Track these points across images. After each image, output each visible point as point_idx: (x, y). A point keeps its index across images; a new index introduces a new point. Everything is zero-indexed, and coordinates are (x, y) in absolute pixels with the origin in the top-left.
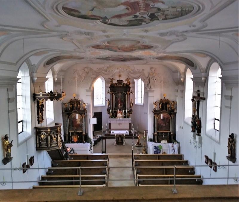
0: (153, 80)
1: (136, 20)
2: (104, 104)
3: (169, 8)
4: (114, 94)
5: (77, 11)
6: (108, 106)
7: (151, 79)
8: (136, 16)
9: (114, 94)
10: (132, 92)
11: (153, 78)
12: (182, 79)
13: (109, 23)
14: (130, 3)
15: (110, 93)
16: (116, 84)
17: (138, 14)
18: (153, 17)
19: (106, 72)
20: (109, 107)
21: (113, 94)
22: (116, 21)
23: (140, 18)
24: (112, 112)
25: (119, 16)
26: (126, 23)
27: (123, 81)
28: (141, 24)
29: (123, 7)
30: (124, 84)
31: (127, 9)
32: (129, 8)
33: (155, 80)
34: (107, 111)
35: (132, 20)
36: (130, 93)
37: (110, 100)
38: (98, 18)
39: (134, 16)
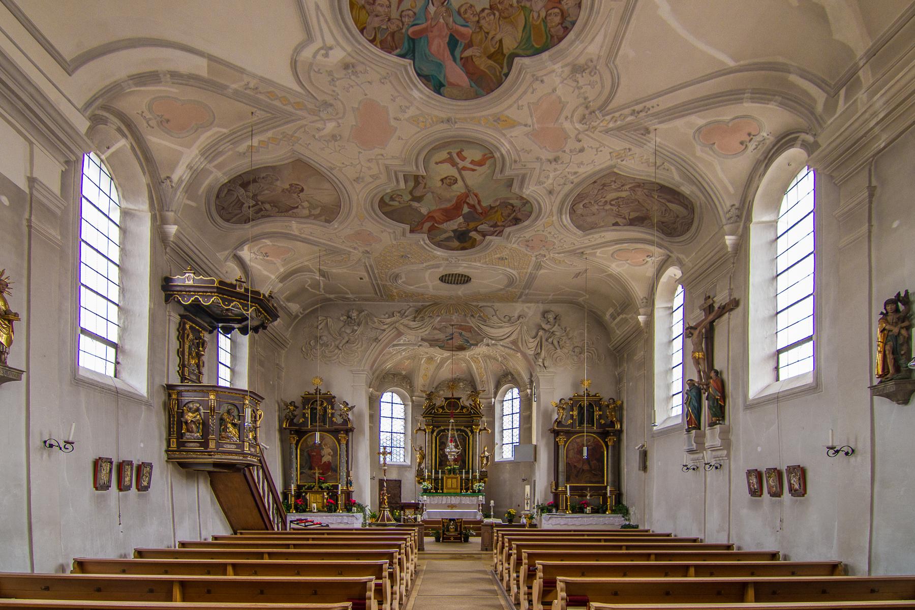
0: (551, 346)
2: (408, 462)
4: (435, 434)
6: (420, 464)
7: (544, 340)
9: (435, 434)
10: (485, 429)
11: (550, 340)
12: (641, 318)
15: (425, 430)
16: (442, 407)
19: (414, 323)
20: (423, 465)
21: (432, 432)
24: (430, 477)
27: (461, 400)
30: (463, 407)
33: (555, 343)
34: (418, 476)
36: (480, 430)
37: (424, 449)
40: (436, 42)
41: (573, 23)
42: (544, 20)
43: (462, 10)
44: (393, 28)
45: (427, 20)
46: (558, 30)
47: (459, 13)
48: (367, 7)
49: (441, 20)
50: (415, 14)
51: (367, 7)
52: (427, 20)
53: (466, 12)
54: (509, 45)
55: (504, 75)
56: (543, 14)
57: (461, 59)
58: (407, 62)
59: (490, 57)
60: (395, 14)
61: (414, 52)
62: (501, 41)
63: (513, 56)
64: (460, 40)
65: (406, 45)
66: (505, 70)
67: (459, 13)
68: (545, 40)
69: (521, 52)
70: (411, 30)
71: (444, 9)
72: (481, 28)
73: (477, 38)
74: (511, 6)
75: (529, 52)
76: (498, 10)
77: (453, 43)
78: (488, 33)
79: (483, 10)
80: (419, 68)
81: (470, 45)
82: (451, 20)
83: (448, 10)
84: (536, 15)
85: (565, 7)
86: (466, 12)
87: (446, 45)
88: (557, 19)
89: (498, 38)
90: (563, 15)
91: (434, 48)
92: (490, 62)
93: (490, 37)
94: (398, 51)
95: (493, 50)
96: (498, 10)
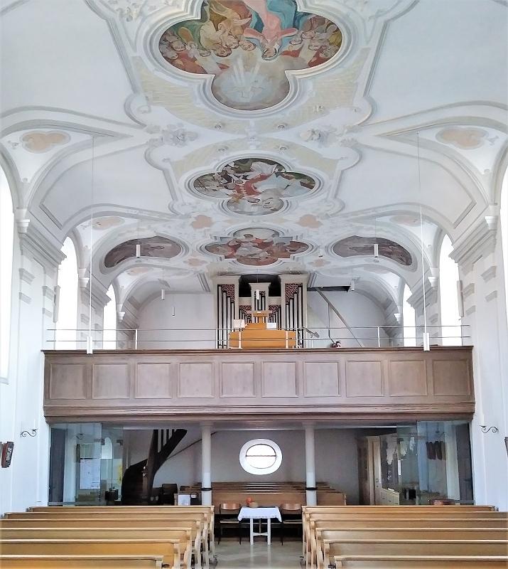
1: (244, 172)
5: (303, 184)
8: (245, 178)
18: (225, 175)
25: (263, 178)
26: (254, 165)
28: (236, 163)
29: (259, 190)
31: (255, 188)
40: (274, 26)
41: (160, 43)
42: (185, 45)
43: (253, 47)
44: (309, 33)
45: (281, 39)
46: (170, 39)
47: (254, 44)
48: (327, 44)
49: (269, 40)
50: (290, 43)
51: (327, 44)
52: (281, 39)
53: (250, 46)
54: (208, 30)
55: (206, 5)
56: (187, 47)
57: (251, 16)
58: (301, 9)
59: (224, 18)
60: (307, 42)
61: (295, 19)
62: (217, 30)
63: (204, 18)
64: (252, 29)
65: (301, 22)
66: (207, 8)
67: (254, 44)
68: (179, 33)
69: (196, 23)
70: (296, 33)
71: (266, 47)
72: (236, 38)
73: (238, 31)
74: (214, 50)
75: (189, 23)
76: (224, 48)
77: (259, 27)
78: (229, 35)
79: (236, 48)
80: (291, 5)
81: (243, 27)
82: (261, 42)
83: (262, 46)
84: (193, 46)
85: (172, 52)
86: (250, 46)
87: (265, 25)
88: (174, 45)
89: (220, 32)
90: (171, 46)
91: (276, 23)
92: (223, 15)
93: (227, 33)
94: (310, 17)
95: (222, 23)
96: (224, 48)
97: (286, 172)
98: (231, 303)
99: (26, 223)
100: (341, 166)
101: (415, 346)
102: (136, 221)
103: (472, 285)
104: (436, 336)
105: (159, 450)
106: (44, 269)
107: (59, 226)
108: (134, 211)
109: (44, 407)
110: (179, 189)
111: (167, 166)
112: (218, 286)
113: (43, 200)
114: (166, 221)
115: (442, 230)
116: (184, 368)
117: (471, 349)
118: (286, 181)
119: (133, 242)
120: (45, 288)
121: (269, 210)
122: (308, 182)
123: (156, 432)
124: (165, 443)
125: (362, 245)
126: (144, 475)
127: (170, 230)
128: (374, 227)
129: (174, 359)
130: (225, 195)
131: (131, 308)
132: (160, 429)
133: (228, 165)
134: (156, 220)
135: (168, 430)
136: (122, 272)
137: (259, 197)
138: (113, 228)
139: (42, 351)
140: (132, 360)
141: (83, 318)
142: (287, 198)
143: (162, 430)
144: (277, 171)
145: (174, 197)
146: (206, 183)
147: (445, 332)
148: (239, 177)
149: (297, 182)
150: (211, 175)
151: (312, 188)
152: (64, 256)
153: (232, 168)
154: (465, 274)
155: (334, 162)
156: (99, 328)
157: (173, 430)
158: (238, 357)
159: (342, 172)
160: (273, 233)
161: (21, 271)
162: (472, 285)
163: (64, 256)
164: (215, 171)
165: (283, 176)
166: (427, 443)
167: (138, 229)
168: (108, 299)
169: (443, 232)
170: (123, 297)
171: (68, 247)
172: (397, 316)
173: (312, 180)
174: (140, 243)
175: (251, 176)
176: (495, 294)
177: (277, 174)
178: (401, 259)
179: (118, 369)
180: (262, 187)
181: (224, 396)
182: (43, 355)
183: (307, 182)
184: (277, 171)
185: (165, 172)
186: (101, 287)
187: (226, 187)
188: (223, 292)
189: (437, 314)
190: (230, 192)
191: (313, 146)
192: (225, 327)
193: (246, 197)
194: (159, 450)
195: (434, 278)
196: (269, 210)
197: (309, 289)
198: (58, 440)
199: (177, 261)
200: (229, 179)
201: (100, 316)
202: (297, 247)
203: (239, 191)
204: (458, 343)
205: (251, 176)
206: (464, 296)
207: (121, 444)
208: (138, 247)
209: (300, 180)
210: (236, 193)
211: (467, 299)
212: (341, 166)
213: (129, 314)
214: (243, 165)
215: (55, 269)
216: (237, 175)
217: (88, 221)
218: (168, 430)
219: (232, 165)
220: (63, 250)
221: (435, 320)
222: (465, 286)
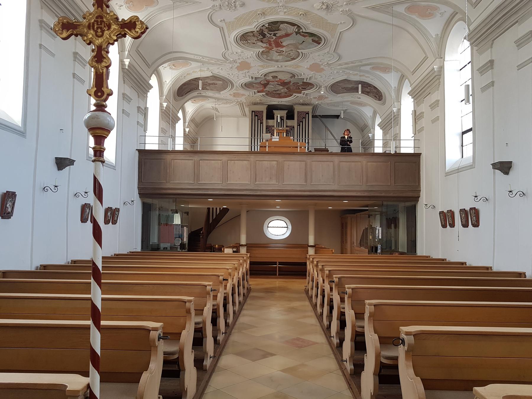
1: (274, 31)
3: (257, 43)
5: (313, 41)
8: (275, 35)
13: (296, 27)
14: (280, 47)
17: (274, 37)
18: (261, 33)
22: (291, 29)
23: (271, 33)
25: (287, 35)
28: (269, 24)
31: (282, 43)
32: (280, 42)
35: (278, 31)
38: (302, 34)
39: (277, 35)
97: (302, 32)
98: (261, 123)
99: (127, 62)
100: (340, 29)
101: (382, 152)
102: (199, 64)
103: (422, 113)
104: (398, 147)
105: (211, 221)
106: (138, 95)
107: (148, 66)
108: (198, 57)
109: (138, 188)
110: (230, 42)
111: (223, 25)
112: (252, 112)
113: (138, 47)
114: (220, 65)
115: (404, 76)
116: (230, 163)
117: (420, 156)
118: (303, 38)
119: (197, 80)
120: (139, 108)
121: (289, 59)
122: (316, 39)
123: (209, 209)
124: (214, 217)
125: (350, 86)
126: (201, 237)
127: (223, 72)
128: (359, 73)
129: (224, 158)
130: (260, 47)
131: (193, 125)
132: (211, 207)
133: (264, 26)
134: (213, 64)
135: (216, 208)
136: (188, 101)
137: (284, 49)
138: (184, 69)
139: (137, 150)
140: (196, 158)
141: (162, 130)
142: (302, 51)
143: (213, 208)
144: (296, 30)
145: (226, 48)
146: (248, 38)
147: (403, 143)
148: (271, 34)
149: (310, 39)
150: (252, 32)
151: (319, 43)
152: (151, 87)
153: (267, 28)
154: (418, 106)
155: (335, 26)
156: (173, 138)
157: (220, 208)
158: (267, 157)
159: (341, 32)
160: (291, 75)
161: (124, 94)
162: (422, 113)
163: (151, 87)
164: (255, 30)
165: (301, 35)
166: (387, 219)
167: (201, 71)
168: (180, 119)
169: (404, 78)
170: (188, 119)
171: (153, 81)
172: (370, 135)
173: (320, 38)
174: (202, 80)
175: (279, 34)
176: (437, 118)
177: (297, 33)
178: (375, 96)
179: (188, 163)
180: (286, 42)
181: (257, 183)
182: (137, 152)
183: (316, 39)
184: (296, 30)
185: (222, 29)
186: (174, 110)
187: (262, 42)
188: (256, 115)
189: (398, 134)
190: (264, 45)
191: (323, 14)
192: (256, 137)
193: (275, 49)
194: (211, 221)
195: (396, 109)
196: (289, 59)
197: (313, 116)
198: (147, 209)
199: (226, 94)
200: (264, 36)
201: (173, 130)
202: (307, 85)
203: (270, 45)
204: (411, 151)
205: (279, 34)
206: (417, 121)
207: (188, 214)
208: (200, 82)
209: (312, 38)
210: (268, 46)
211: (419, 123)
212: (340, 29)
213: (192, 130)
214: (274, 26)
215: (145, 95)
216: (269, 32)
217: (167, 64)
218: (216, 208)
219: (267, 25)
220: (151, 82)
221: (397, 138)
222: (417, 114)
